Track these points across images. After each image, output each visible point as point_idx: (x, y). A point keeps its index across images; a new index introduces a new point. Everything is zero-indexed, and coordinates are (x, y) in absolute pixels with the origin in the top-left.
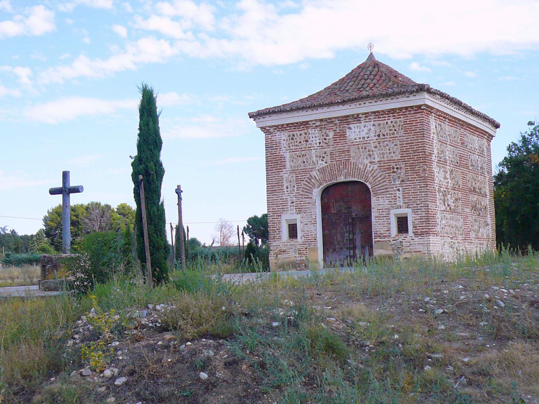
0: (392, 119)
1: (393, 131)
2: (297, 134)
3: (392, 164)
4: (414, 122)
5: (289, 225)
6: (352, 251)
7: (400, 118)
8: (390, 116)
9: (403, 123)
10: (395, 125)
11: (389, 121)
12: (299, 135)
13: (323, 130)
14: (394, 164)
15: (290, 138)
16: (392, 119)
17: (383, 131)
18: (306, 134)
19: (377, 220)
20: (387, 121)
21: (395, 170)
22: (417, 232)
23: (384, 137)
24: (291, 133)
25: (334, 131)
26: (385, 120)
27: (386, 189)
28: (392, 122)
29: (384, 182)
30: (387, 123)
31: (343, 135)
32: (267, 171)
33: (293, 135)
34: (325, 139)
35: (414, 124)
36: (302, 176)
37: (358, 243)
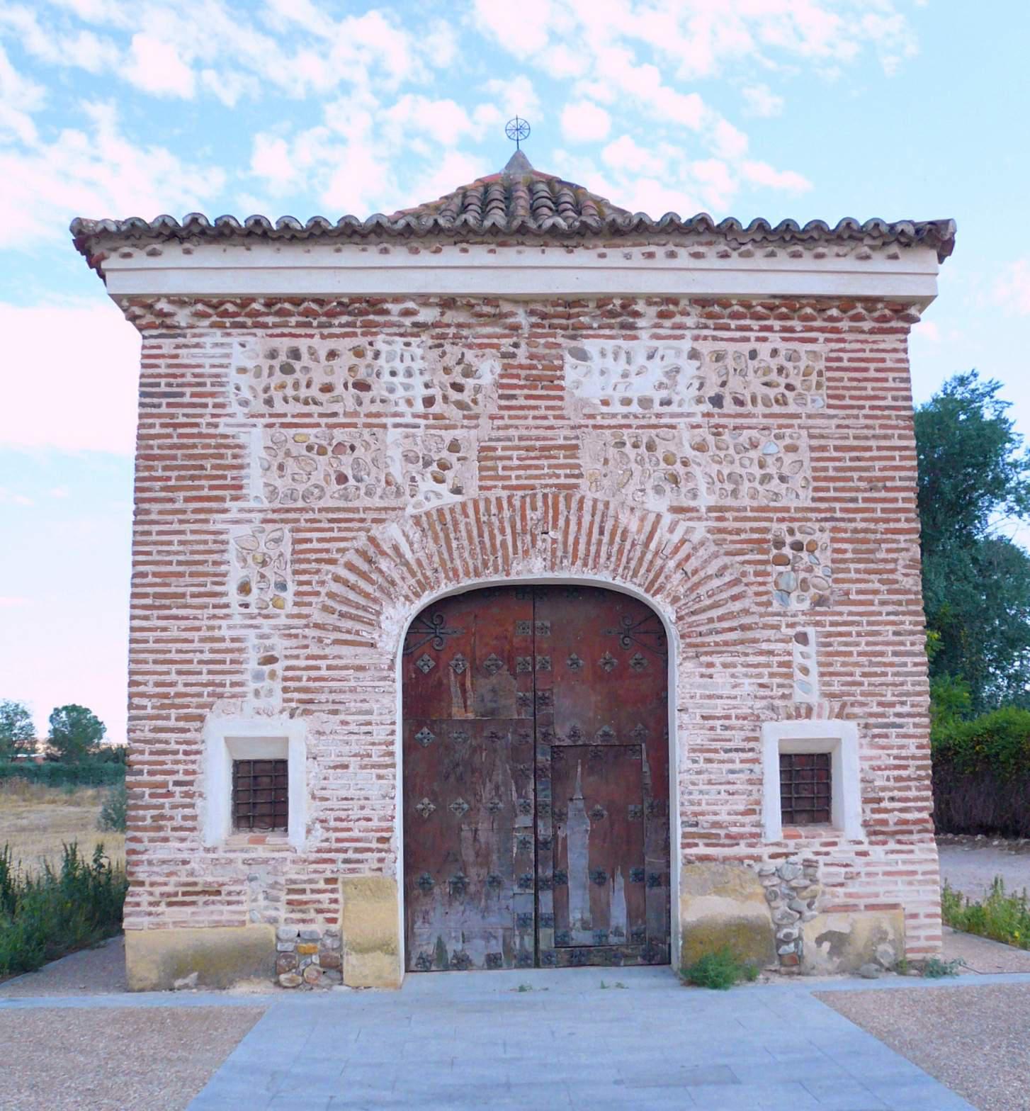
0: (775, 340)
1: (782, 389)
2: (312, 352)
3: (775, 526)
4: (872, 366)
5: (237, 765)
6: (547, 898)
7: (814, 340)
8: (769, 329)
9: (822, 365)
10: (789, 365)
11: (764, 350)
12: (322, 354)
13: (448, 347)
14: (784, 526)
15: (276, 363)
16: (775, 340)
17: (735, 383)
18: (359, 353)
19: (702, 765)
20: (753, 345)
21: (787, 551)
22: (884, 822)
23: (739, 409)
24: (284, 344)
25: (504, 355)
26: (747, 340)
27: (744, 628)
28: (775, 353)
29: (735, 598)
30: (753, 355)
31: (545, 380)
32: (137, 501)
33: (295, 354)
34: (458, 388)
35: (872, 374)
36: (320, 538)
37: (578, 860)
